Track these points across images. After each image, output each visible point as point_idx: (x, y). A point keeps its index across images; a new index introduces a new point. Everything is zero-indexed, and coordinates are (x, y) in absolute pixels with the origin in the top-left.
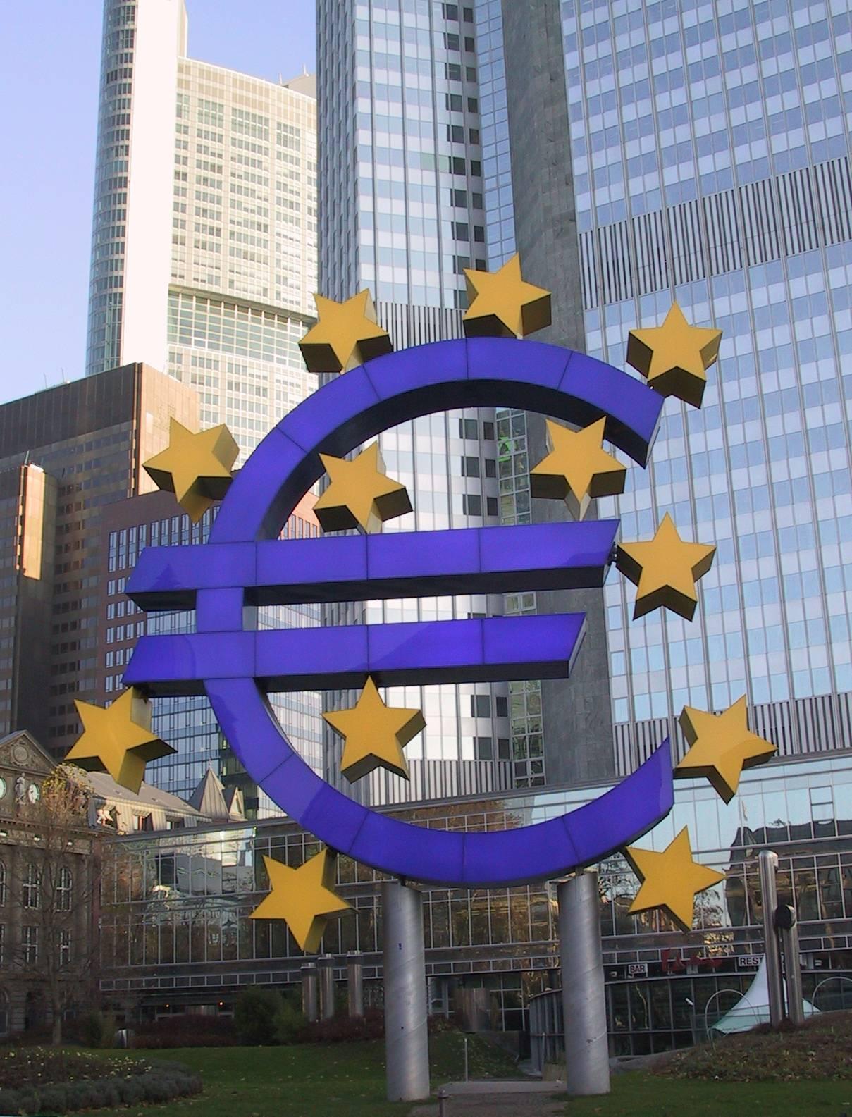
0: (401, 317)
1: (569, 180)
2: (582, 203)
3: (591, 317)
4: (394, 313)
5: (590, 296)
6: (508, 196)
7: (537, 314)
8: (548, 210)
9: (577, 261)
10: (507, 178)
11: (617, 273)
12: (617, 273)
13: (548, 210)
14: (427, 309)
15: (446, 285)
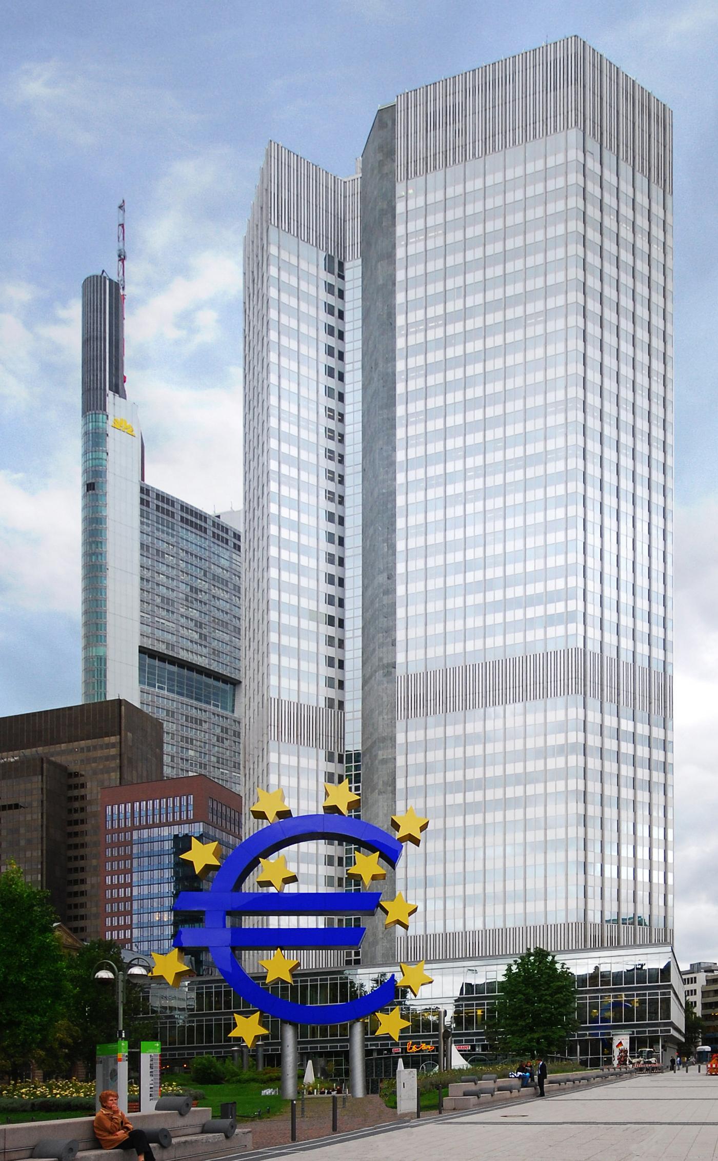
0: (294, 710)
1: (394, 644)
2: (400, 658)
3: (400, 725)
4: (289, 707)
5: (401, 713)
6: (359, 644)
7: (354, 806)
8: (381, 659)
9: (394, 695)
10: (359, 632)
11: (416, 702)
12: (416, 702)
13: (381, 659)
14: (309, 707)
15: (320, 693)
